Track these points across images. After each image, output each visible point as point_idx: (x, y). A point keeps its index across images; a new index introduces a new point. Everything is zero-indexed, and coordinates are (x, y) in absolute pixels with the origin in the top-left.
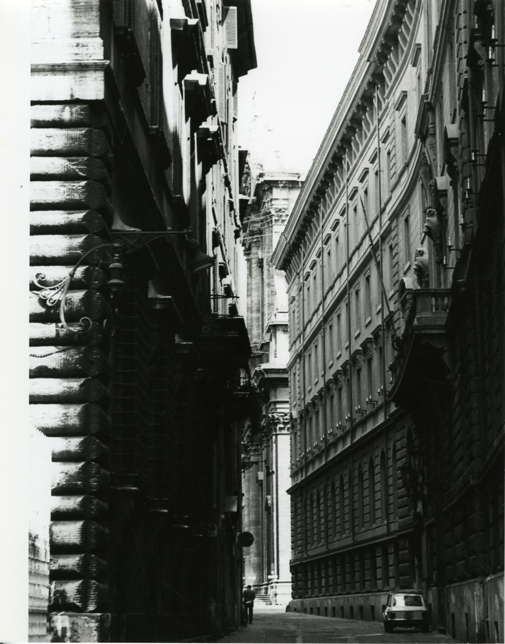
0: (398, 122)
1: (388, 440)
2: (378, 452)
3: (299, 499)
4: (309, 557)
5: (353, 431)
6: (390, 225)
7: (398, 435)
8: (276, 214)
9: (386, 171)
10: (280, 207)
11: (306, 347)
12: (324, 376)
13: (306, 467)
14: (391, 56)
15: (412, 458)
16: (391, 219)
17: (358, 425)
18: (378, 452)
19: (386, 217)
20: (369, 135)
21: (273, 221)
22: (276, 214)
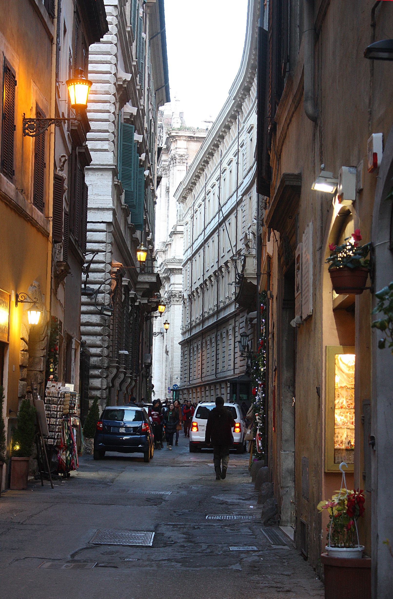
0: (249, 140)
1: (217, 331)
2: (231, 327)
3: (186, 349)
4: (191, 384)
5: (218, 312)
6: (242, 198)
7: (241, 320)
8: (179, 158)
9: (242, 163)
10: (182, 153)
11: (193, 255)
12: (218, 262)
13: (191, 330)
14: (246, 100)
15: (242, 338)
16: (243, 195)
17: (193, 327)
18: (231, 327)
19: (240, 193)
20: (227, 148)
21: (177, 163)
22: (179, 158)
